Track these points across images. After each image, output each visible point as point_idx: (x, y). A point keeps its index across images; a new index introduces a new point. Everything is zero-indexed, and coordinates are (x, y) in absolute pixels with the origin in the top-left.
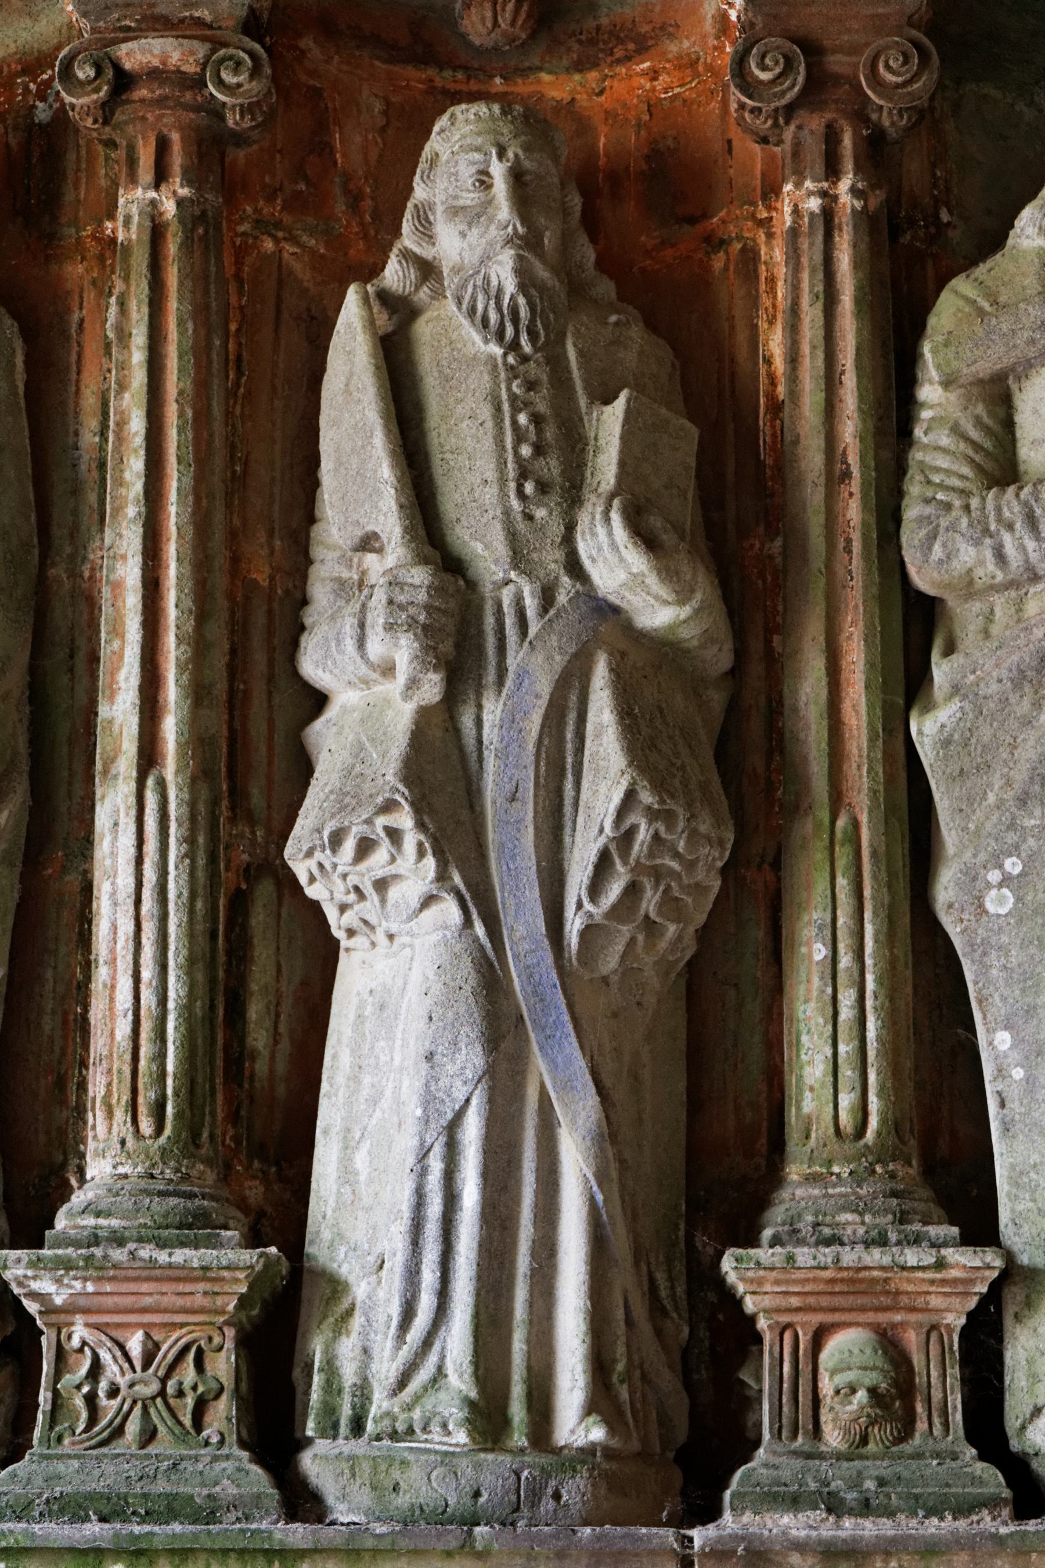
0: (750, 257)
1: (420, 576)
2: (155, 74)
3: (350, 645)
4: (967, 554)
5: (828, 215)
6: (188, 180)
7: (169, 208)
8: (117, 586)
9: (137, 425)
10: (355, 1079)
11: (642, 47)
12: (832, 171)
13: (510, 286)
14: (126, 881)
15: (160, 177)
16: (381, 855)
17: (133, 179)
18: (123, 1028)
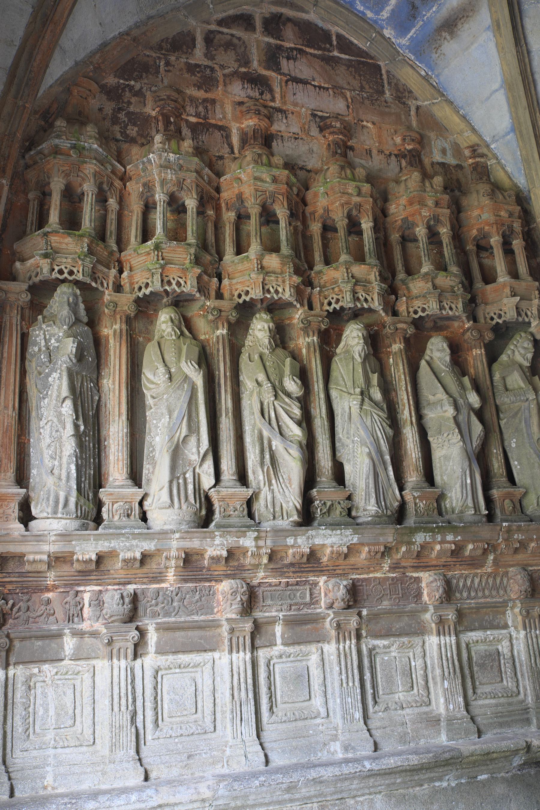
0: (466, 359)
1: (451, 399)
2: (401, 329)
3: (439, 408)
4: (506, 399)
5: (481, 353)
6: (405, 342)
7: (402, 347)
8: (402, 400)
9: (403, 377)
10: (441, 467)
11: (445, 330)
12: (481, 349)
13: (448, 361)
14: (411, 440)
15: (400, 343)
16: (450, 436)
17: (395, 343)
18: (414, 460)
